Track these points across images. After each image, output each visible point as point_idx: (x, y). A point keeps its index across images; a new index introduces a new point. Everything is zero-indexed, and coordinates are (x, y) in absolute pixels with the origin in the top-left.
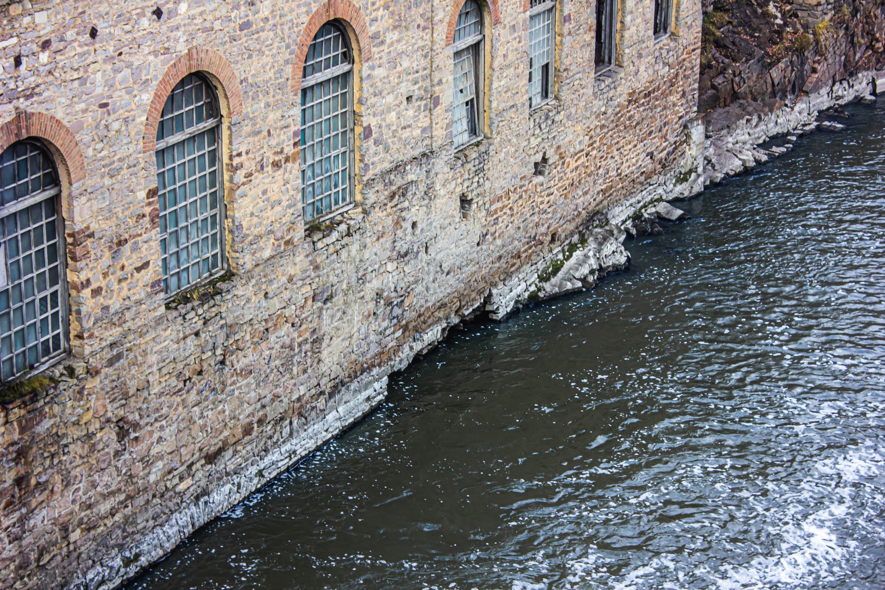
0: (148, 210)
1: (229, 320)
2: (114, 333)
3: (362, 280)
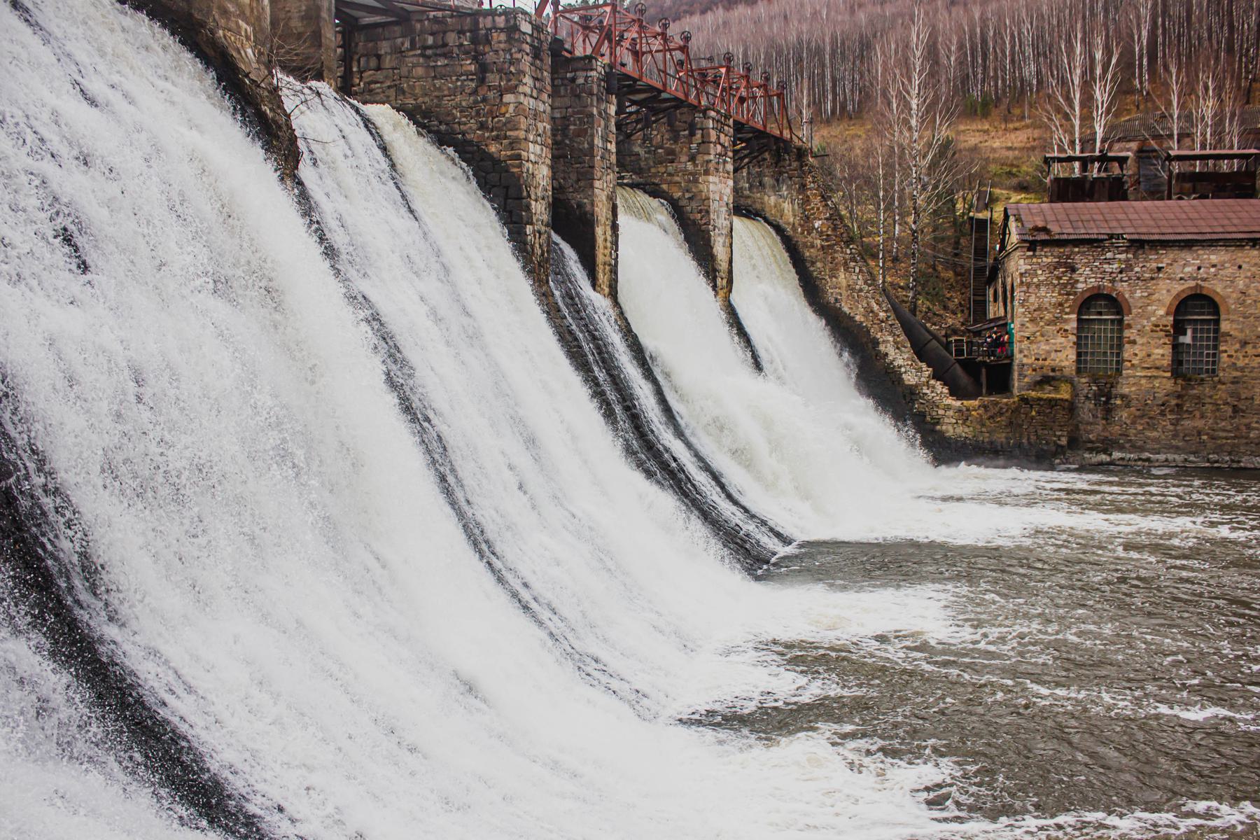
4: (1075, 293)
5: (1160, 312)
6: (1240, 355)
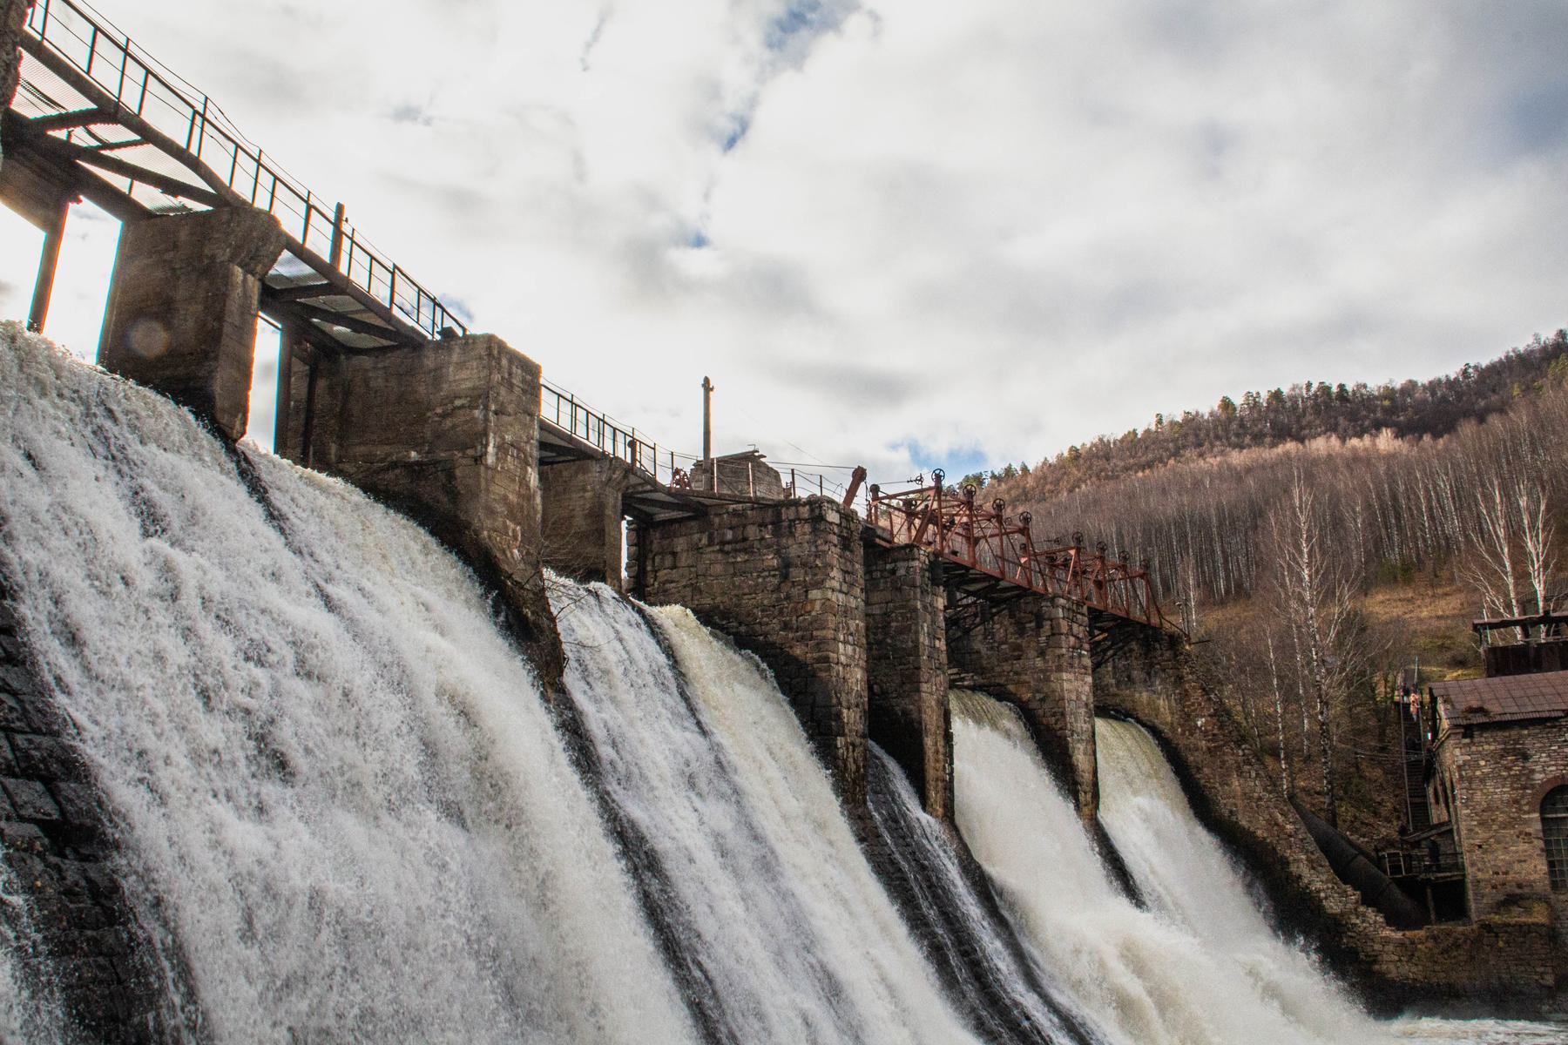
4: (1533, 787)
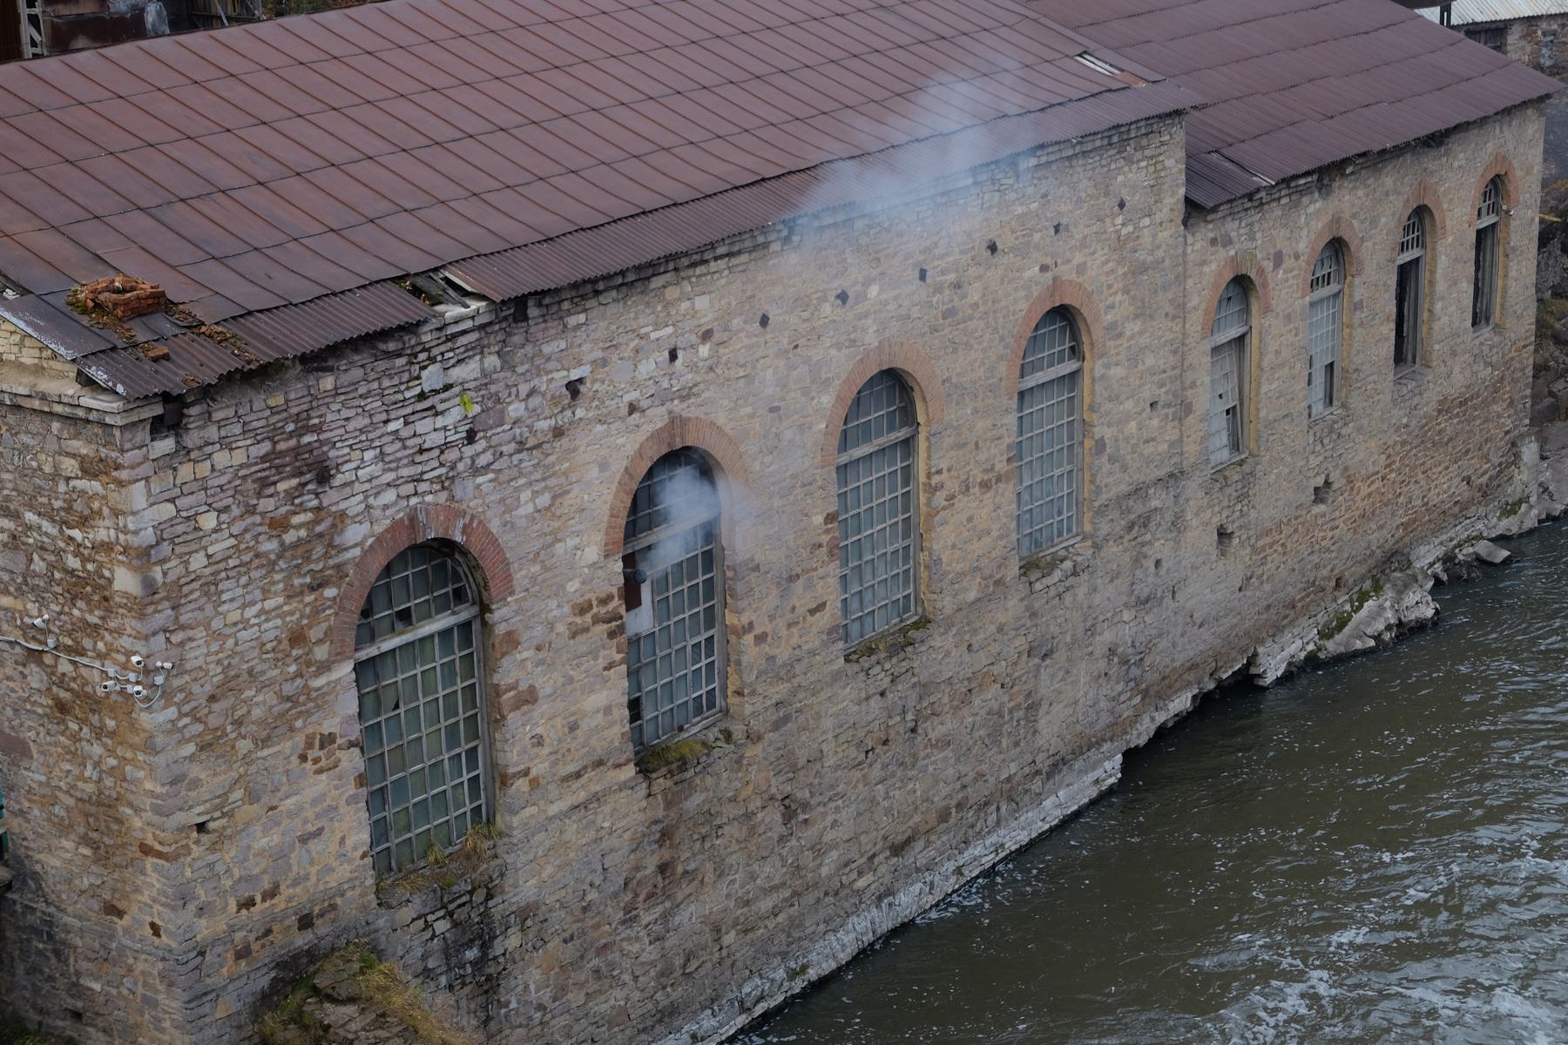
0: (825, 539)
1: (924, 678)
2: (780, 690)
3: (1091, 631)
5: (589, 558)
6: (780, 622)
